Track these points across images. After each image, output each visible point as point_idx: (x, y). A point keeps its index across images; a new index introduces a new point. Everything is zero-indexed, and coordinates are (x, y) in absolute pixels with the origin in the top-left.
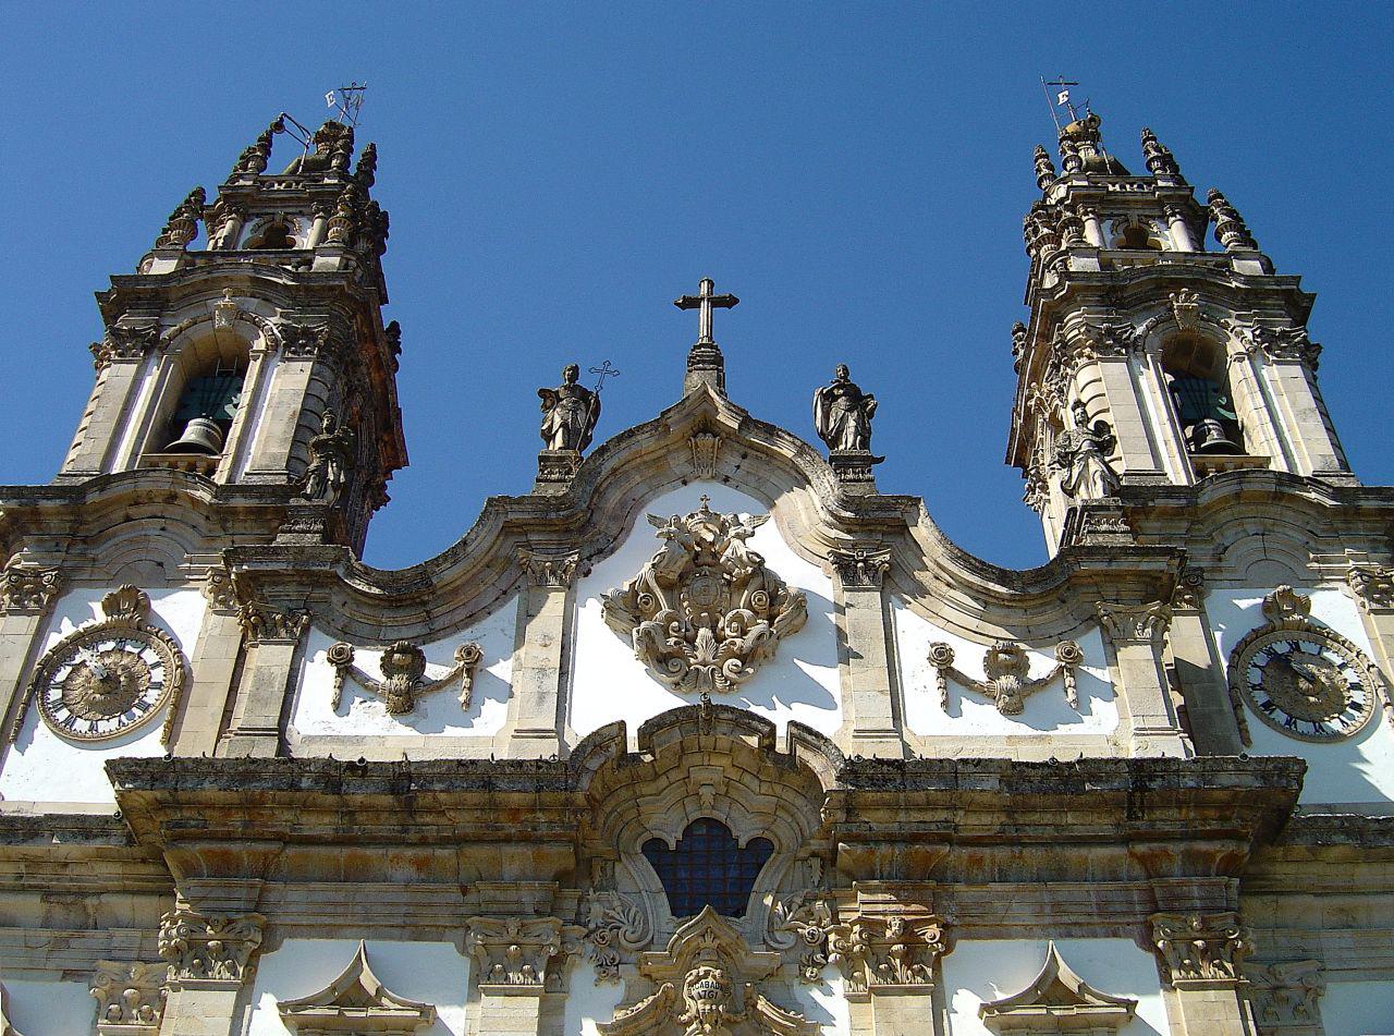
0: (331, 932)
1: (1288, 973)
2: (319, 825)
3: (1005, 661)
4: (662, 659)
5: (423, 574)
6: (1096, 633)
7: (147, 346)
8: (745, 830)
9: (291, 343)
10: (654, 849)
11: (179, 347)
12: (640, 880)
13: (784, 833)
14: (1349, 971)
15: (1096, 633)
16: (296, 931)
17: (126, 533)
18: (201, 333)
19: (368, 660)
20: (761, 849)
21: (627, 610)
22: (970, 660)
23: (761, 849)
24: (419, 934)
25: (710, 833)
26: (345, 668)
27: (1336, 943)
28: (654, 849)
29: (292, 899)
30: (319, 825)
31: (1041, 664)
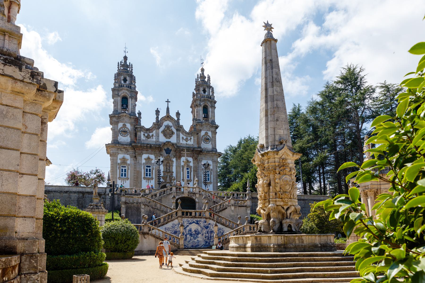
0: (146, 154)
1: (200, 160)
2: (145, 147)
3: (187, 139)
4: (165, 135)
5: (149, 128)
6: (193, 137)
7: (118, 95)
8: (170, 149)
9: (132, 97)
10: (165, 149)
11: (121, 96)
12: (164, 151)
13: (172, 149)
14: (204, 160)
15: (193, 137)
16: (144, 154)
17: (122, 118)
18: (123, 94)
19: (146, 135)
20: (171, 150)
21: (163, 132)
22: (185, 137)
23: (171, 150)
24: (151, 154)
25: (168, 148)
26: (144, 135)
27: (204, 158)
28: (165, 149)
29: (144, 152)
30: (145, 147)
31: (189, 138)
